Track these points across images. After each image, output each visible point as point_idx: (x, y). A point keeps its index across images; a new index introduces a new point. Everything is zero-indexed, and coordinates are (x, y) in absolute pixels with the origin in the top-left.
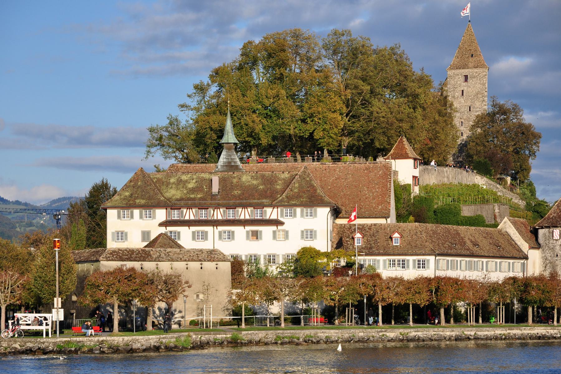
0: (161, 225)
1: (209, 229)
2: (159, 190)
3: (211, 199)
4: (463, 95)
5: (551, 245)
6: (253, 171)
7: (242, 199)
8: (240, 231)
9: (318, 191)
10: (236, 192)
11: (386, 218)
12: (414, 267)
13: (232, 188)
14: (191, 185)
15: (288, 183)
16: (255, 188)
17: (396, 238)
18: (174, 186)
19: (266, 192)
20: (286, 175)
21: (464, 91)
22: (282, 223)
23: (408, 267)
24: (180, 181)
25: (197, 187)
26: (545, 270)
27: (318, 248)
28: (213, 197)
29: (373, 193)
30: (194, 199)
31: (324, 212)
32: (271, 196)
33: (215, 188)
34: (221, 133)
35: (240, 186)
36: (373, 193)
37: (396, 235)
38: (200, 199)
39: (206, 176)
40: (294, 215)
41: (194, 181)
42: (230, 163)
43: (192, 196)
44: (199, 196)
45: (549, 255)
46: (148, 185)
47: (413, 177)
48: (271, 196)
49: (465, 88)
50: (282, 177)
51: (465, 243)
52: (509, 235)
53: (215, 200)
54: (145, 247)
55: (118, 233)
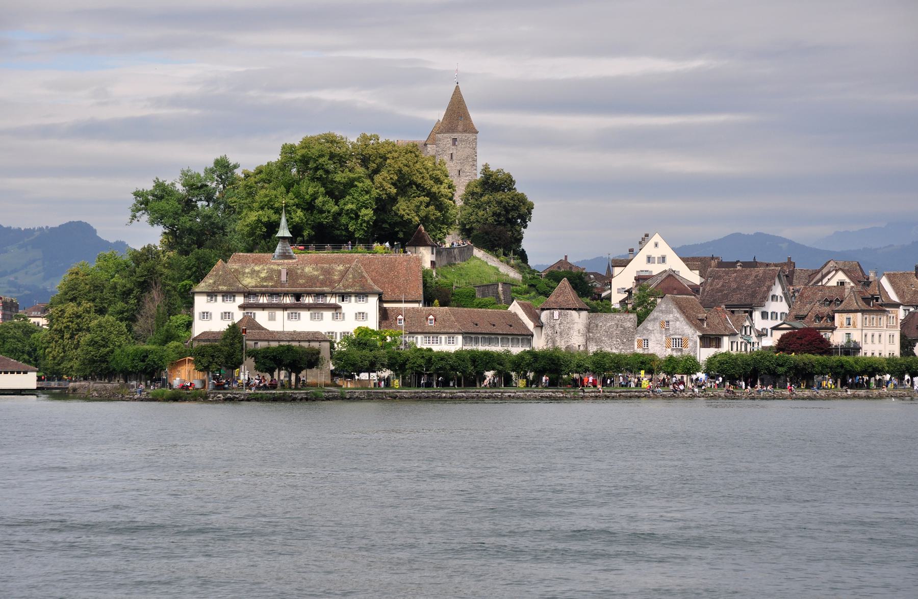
0: (241, 307)
1: (279, 314)
6: (310, 263)
8: (305, 315)
13: (298, 277)
14: (263, 275)
15: (343, 274)
16: (317, 277)
17: (431, 320)
20: (341, 268)
22: (340, 307)
27: (371, 328)
28: (282, 285)
30: (267, 286)
31: (373, 301)
34: (273, 227)
35: (303, 275)
37: (431, 317)
38: (272, 286)
39: (275, 267)
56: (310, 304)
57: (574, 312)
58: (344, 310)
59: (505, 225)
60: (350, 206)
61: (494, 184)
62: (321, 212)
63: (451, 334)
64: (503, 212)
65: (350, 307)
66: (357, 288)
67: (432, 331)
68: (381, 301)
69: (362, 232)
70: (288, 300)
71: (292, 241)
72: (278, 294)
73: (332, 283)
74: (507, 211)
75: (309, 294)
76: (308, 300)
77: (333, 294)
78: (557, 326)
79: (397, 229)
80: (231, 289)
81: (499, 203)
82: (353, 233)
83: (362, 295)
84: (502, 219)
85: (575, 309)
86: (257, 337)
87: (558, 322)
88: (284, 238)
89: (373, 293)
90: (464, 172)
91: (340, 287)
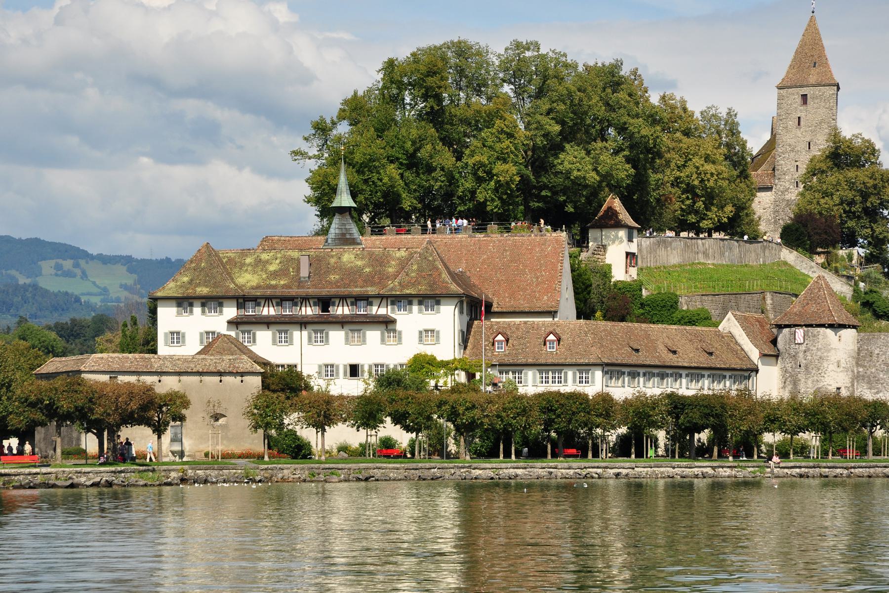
2: (229, 274)
3: (299, 287)
4: (799, 124)
5: (792, 352)
7: (338, 287)
9: (443, 276)
10: (333, 277)
11: (553, 314)
12: (574, 381)
14: (272, 268)
15: (403, 264)
16: (359, 270)
17: (552, 342)
18: (250, 268)
19: (373, 277)
20: (403, 253)
21: (802, 119)
22: (393, 322)
23: (566, 381)
24: (259, 262)
25: (280, 270)
26: (784, 387)
28: (300, 283)
29: (537, 278)
30: (275, 287)
32: (379, 283)
33: (304, 272)
35: (339, 268)
36: (537, 278)
38: (283, 286)
39: (295, 254)
40: (411, 311)
41: (278, 261)
42: (343, 234)
43: (273, 282)
44: (282, 282)
45: (790, 365)
46: (214, 268)
47: (628, 254)
48: (379, 283)
49: (802, 115)
50: (397, 255)
51: (655, 349)
52: (733, 337)
53: (303, 287)
54: (199, 353)
55: (172, 333)
56: (344, 316)
57: (829, 331)
58: (399, 327)
59: (859, 218)
60: (477, 158)
61: (843, 156)
62: (430, 169)
63: (584, 367)
64: (858, 199)
65: (411, 321)
66: (423, 289)
67: (550, 361)
68: (475, 308)
69: (497, 202)
70: (309, 311)
71: (354, 213)
72: (293, 300)
73: (383, 278)
74: (865, 196)
75: (343, 299)
76: (342, 310)
77: (382, 298)
78: (801, 355)
79: (562, 198)
80: (219, 292)
81: (851, 185)
82: (484, 204)
83: (431, 299)
84: (857, 208)
85: (831, 326)
86: (116, 367)
87: (803, 348)
88: (342, 210)
89: (450, 296)
90: (816, 144)
91: (393, 286)
